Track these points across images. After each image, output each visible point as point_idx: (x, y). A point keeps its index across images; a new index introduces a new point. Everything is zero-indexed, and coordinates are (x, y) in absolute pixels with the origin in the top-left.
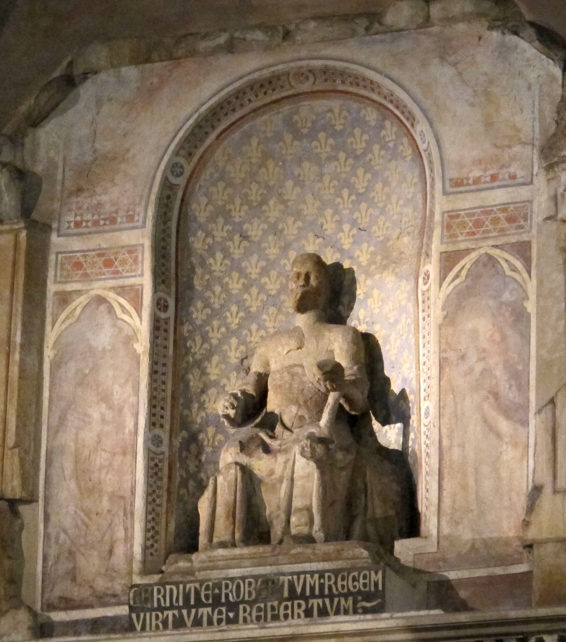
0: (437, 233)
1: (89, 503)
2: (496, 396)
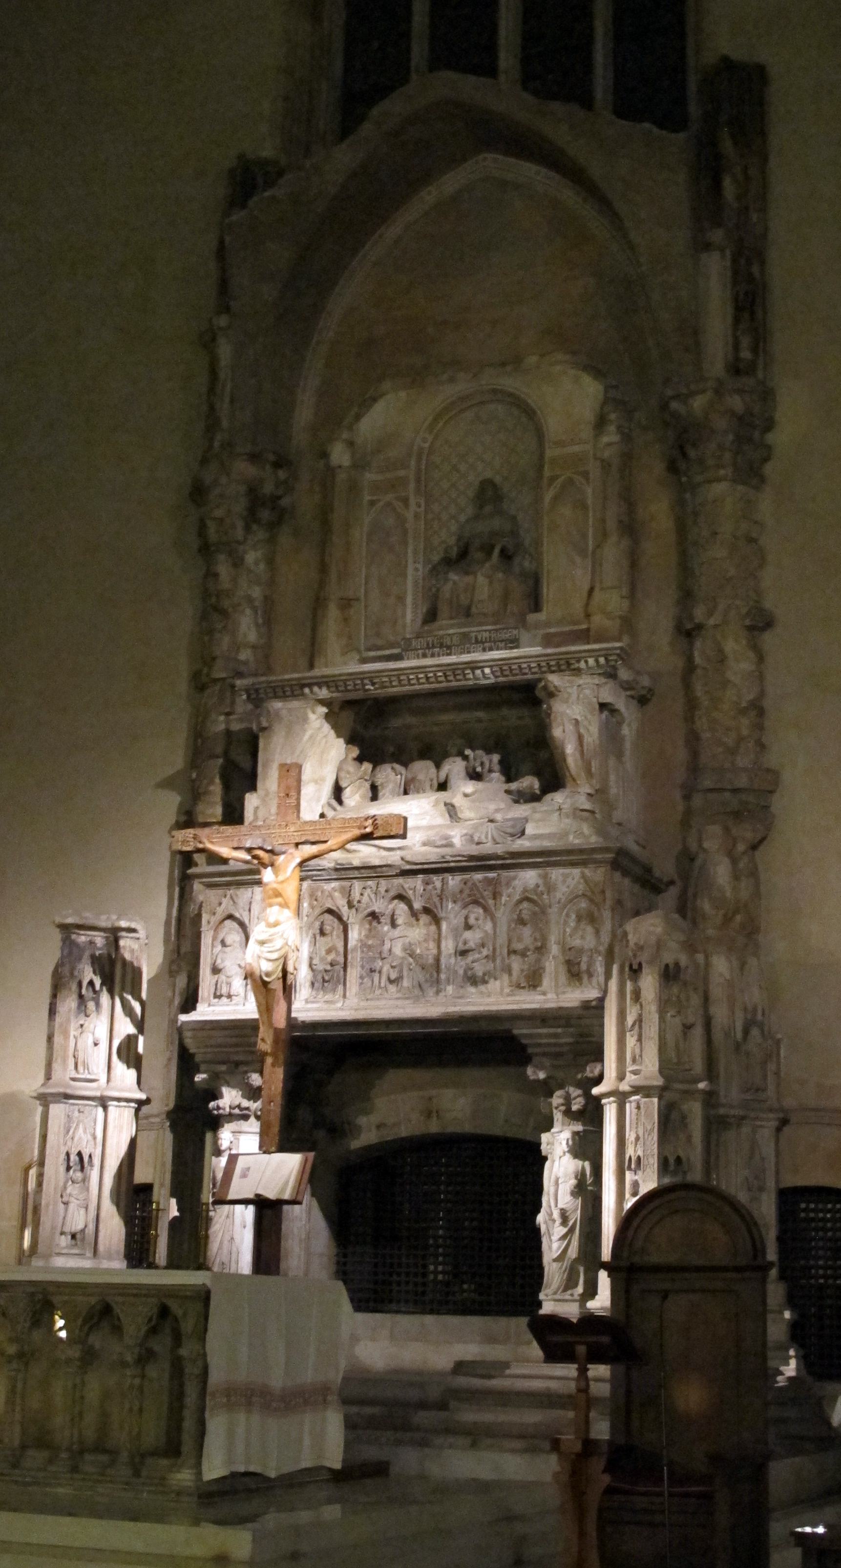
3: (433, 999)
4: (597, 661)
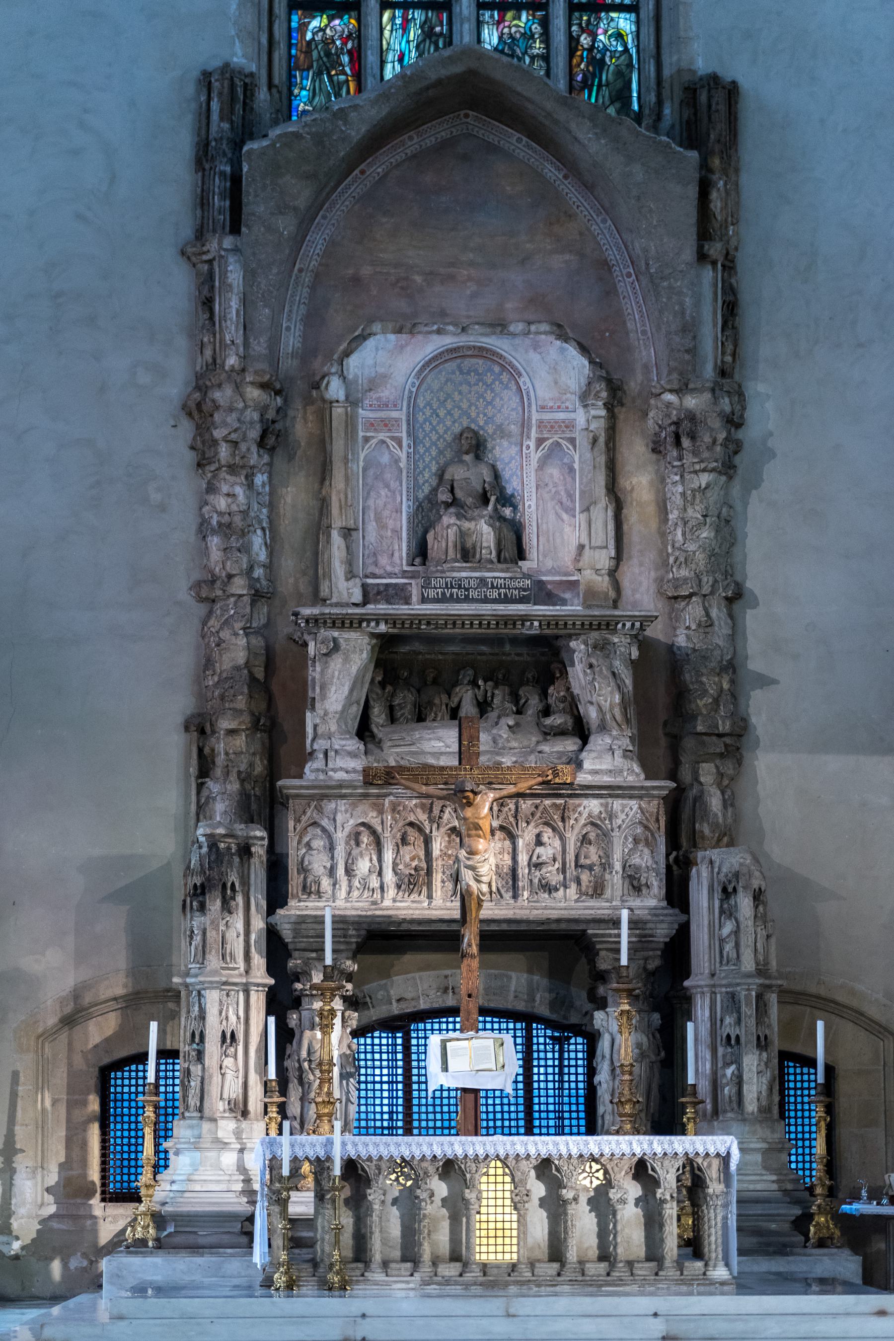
0: (534, 430)
1: (382, 533)
2: (561, 503)
3: (512, 901)
4: (633, 625)
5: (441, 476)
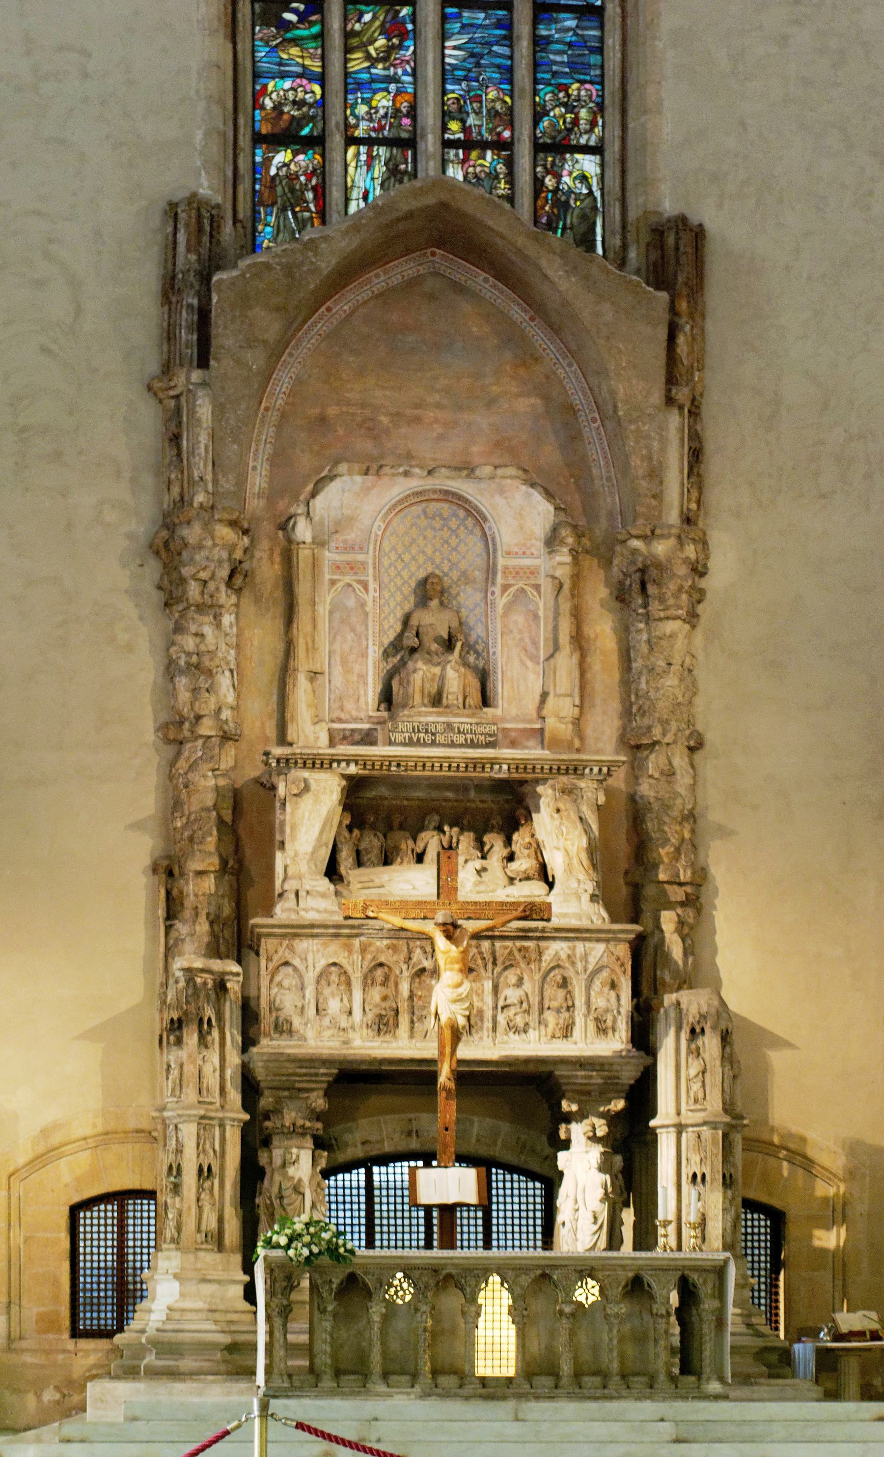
2: (526, 650)
4: (600, 770)
5: (406, 621)
